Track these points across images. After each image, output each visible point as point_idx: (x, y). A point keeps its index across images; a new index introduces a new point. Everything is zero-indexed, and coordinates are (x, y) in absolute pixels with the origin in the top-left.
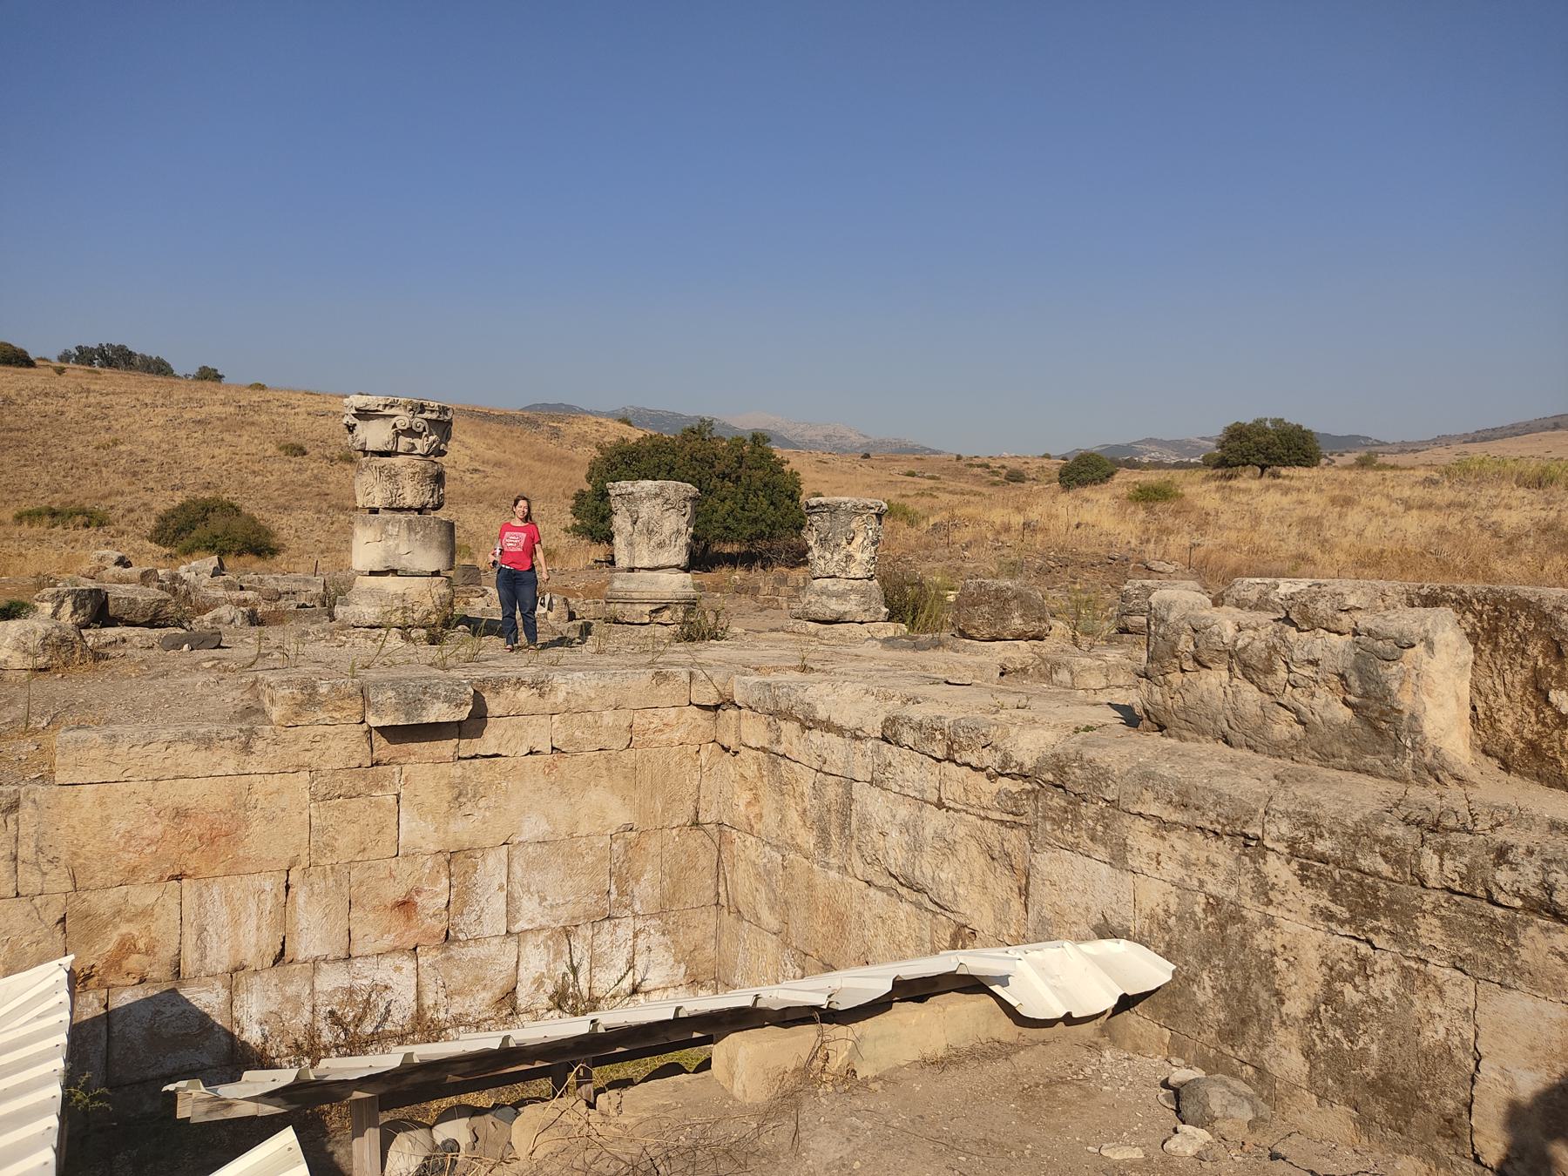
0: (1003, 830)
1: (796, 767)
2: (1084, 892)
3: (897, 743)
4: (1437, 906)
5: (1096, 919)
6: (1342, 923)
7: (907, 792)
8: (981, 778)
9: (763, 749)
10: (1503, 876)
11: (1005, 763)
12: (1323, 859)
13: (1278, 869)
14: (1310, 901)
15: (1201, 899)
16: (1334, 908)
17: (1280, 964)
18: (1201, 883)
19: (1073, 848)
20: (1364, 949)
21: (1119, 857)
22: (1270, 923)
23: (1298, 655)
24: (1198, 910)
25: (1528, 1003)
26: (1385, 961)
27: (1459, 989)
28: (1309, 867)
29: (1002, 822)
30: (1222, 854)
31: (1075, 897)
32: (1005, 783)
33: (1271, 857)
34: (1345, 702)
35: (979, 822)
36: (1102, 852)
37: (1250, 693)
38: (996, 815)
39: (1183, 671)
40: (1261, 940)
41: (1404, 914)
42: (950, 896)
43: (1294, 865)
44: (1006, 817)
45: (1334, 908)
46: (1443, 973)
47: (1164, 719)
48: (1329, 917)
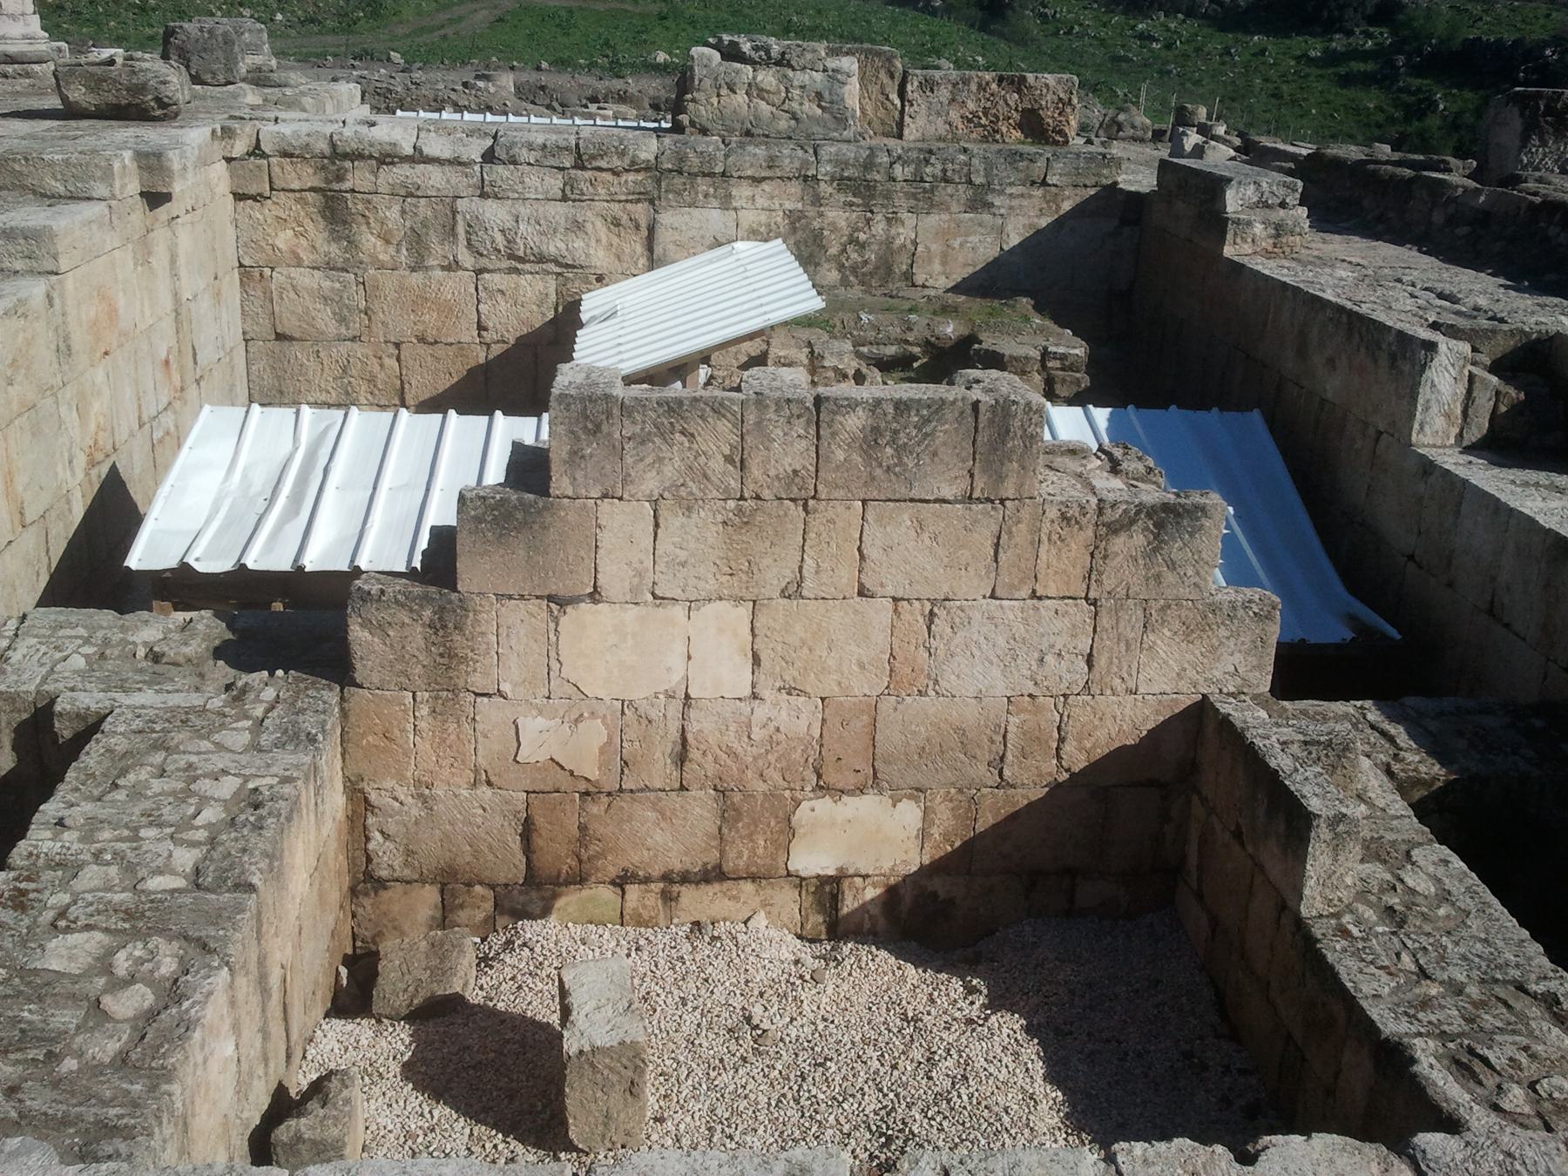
0: (629, 206)
1: (375, 198)
2: (700, 228)
3: (514, 162)
4: (902, 188)
5: (709, 240)
6: (858, 206)
7: (527, 196)
8: (608, 176)
9: (312, 189)
10: (928, 170)
11: (633, 163)
12: (849, 179)
13: (825, 189)
14: (842, 199)
15: (781, 214)
16: (855, 200)
17: (825, 233)
18: (781, 205)
20: (869, 215)
21: (726, 203)
22: (821, 215)
23: (796, 83)
24: (779, 219)
25: (937, 217)
26: (879, 217)
27: (910, 219)
28: (842, 182)
29: (627, 201)
30: (795, 188)
31: (694, 232)
32: (631, 177)
33: (822, 184)
34: (819, 106)
35: (606, 204)
36: (715, 203)
37: (763, 104)
38: (623, 198)
39: (719, 95)
40: (816, 224)
41: (888, 196)
42: (583, 258)
43: (835, 184)
44: (630, 197)
45: (855, 200)
46: (904, 215)
47: (709, 125)
48: (851, 204)
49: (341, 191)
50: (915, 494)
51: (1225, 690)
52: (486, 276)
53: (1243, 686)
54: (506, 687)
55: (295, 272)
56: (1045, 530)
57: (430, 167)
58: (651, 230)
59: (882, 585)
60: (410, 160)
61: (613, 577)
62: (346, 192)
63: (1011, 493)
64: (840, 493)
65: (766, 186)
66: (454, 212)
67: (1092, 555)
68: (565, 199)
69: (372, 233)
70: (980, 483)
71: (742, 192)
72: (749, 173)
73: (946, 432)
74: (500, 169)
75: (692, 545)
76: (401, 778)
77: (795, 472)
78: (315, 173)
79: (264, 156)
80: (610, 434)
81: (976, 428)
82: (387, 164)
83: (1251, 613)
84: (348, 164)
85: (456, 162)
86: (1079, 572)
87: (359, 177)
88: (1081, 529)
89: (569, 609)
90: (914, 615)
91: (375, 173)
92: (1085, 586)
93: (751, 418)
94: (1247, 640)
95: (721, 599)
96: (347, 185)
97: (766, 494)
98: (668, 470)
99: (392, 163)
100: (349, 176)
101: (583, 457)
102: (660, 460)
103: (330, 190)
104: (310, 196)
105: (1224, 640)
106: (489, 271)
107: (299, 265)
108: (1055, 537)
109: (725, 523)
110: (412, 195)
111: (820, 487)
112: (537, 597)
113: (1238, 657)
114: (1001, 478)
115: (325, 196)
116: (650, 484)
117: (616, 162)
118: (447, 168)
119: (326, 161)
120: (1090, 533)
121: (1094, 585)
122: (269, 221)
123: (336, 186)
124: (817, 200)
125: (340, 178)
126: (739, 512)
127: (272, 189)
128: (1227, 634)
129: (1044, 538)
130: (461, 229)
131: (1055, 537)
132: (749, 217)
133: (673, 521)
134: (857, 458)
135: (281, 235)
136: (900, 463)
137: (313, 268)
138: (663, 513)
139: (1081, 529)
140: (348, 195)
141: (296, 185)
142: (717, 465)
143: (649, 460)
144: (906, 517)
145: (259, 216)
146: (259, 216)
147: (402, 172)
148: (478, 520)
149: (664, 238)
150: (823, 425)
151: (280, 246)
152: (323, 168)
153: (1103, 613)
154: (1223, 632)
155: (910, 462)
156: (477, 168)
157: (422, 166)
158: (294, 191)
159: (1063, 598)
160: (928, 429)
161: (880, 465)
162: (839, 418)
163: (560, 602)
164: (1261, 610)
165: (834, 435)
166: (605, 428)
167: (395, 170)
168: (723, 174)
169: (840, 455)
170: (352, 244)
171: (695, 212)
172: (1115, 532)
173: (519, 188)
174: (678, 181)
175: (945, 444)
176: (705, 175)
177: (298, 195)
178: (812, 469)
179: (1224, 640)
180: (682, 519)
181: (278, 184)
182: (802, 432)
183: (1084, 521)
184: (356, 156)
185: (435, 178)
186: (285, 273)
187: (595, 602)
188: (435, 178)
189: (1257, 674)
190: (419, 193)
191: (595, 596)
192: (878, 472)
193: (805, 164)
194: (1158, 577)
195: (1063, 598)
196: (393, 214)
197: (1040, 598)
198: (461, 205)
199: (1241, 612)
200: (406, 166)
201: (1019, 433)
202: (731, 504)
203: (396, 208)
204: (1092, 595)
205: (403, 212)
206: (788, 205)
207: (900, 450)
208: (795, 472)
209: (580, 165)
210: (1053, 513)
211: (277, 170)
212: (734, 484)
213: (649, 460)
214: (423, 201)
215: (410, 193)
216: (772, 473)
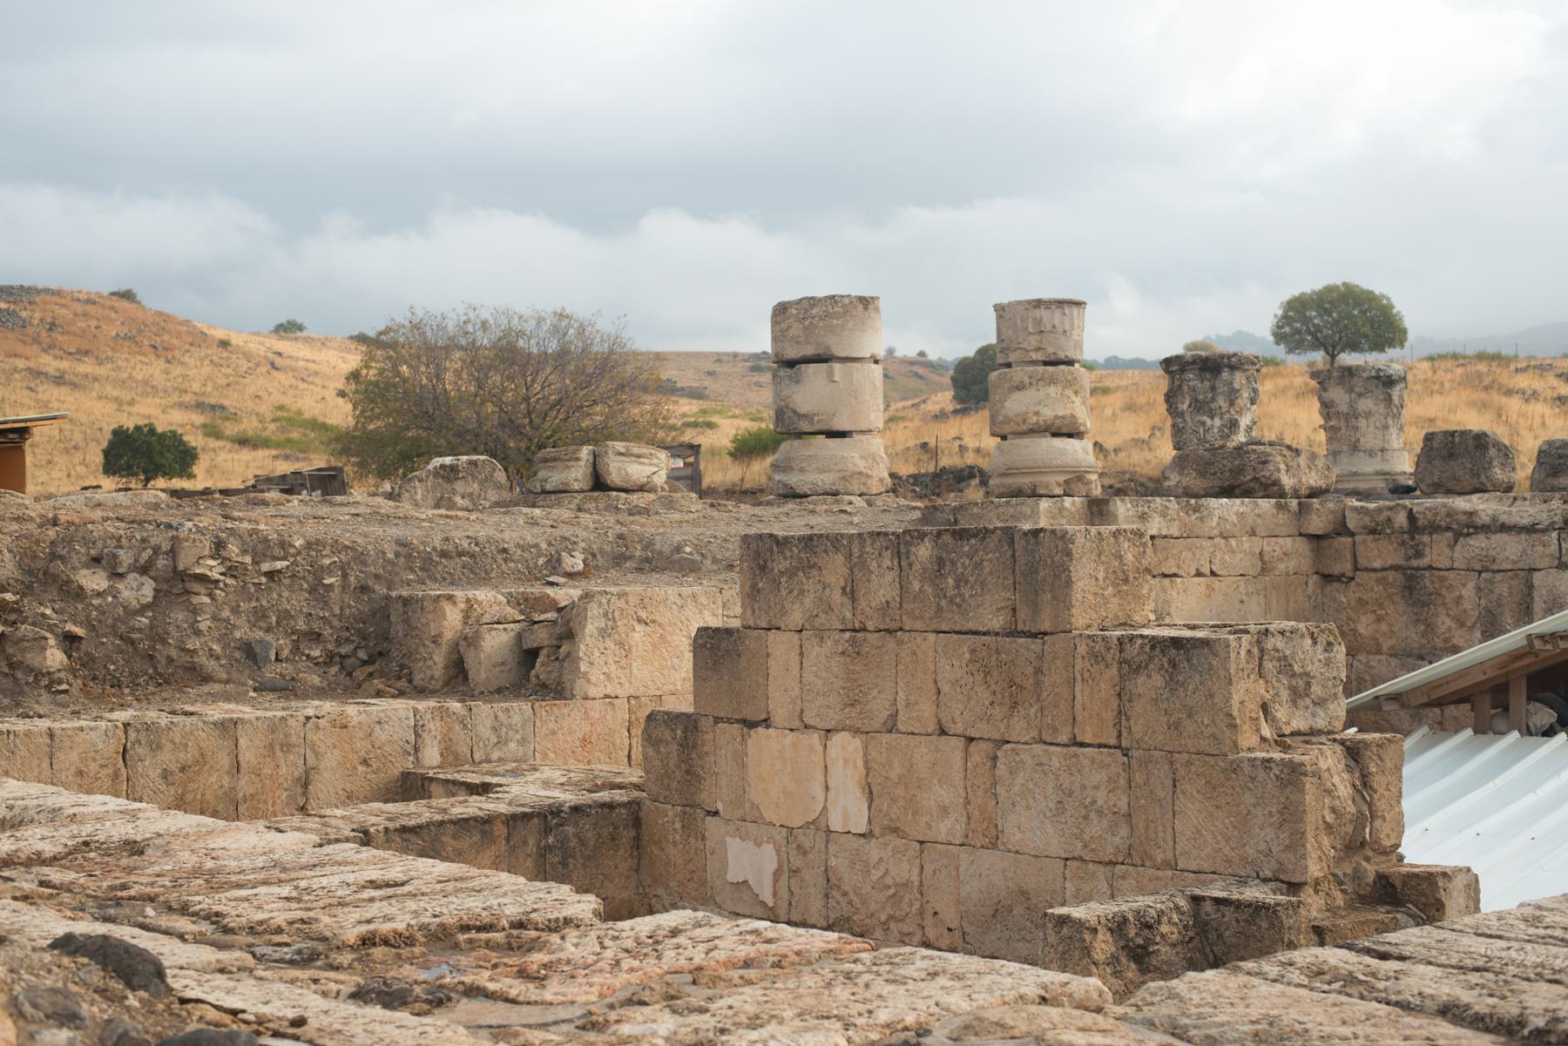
1: (1451, 575)
9: (1395, 568)
49: (1418, 569)
50: (971, 626)
51: (1261, 874)
53: (1278, 870)
54: (720, 806)
55: (1374, 660)
56: (1078, 668)
57: (1505, 537)
59: (954, 723)
60: (1486, 529)
61: (780, 704)
62: (1424, 569)
63: (1046, 626)
64: (918, 625)
66: (1531, 587)
67: (1119, 695)
69: (1448, 615)
70: (1023, 613)
73: (991, 561)
75: (824, 674)
76: (667, 888)
77: (887, 602)
78: (1395, 550)
79: (1352, 534)
80: (772, 569)
81: (1013, 555)
83: (1272, 775)
84: (1426, 539)
85: (1531, 529)
86: (1109, 715)
87: (1437, 551)
88: (1107, 666)
89: (752, 732)
90: (979, 752)
91: (1452, 547)
92: (1115, 733)
93: (855, 550)
94: (1273, 810)
95: (843, 729)
96: (1425, 561)
97: (870, 625)
98: (808, 601)
99: (1468, 535)
100: (1427, 550)
101: (758, 590)
102: (802, 592)
103: (1410, 568)
104: (1391, 575)
105: (1252, 809)
107: (1379, 652)
108: (1087, 675)
109: (843, 653)
110: (1487, 570)
111: (904, 617)
112: (738, 721)
113: (1269, 833)
114: (1035, 608)
115: (1404, 574)
116: (796, 617)
118: (1523, 536)
119: (1406, 536)
120: (1114, 670)
121: (1124, 733)
122: (1353, 603)
123: (1415, 563)
125: (1419, 554)
126: (853, 639)
127: (1356, 568)
128: (1252, 800)
129: (1078, 676)
131: (1087, 675)
133: (815, 651)
134: (928, 589)
135: (1363, 619)
136: (961, 595)
137: (1391, 655)
138: (806, 644)
139: (1107, 666)
140: (1427, 573)
141: (1377, 564)
142: (837, 597)
143: (795, 592)
144: (965, 649)
145: (1343, 599)
146: (1343, 599)
147: (1479, 542)
148: (704, 646)
150: (903, 557)
151: (1362, 631)
152: (1403, 543)
153: (1134, 762)
154: (1249, 799)
155: (966, 592)
156: (1555, 535)
157: (1498, 536)
158: (1374, 570)
159: (1100, 746)
160: (976, 559)
161: (945, 597)
162: (913, 549)
163: (751, 724)
164: (1282, 771)
165: (910, 565)
166: (769, 564)
167: (1471, 542)
169: (916, 586)
170: (1430, 628)
172: (1137, 671)
175: (991, 573)
177: (1380, 575)
178: (898, 599)
179: (1252, 809)
180: (818, 649)
181: (1363, 562)
182: (889, 563)
183: (1109, 658)
184: (1434, 528)
185: (1509, 549)
186: (1364, 660)
187: (768, 727)
189: (1291, 856)
190: (1495, 567)
191: (766, 722)
192: (943, 603)
194: (1177, 726)
195: (1100, 746)
196: (1468, 592)
197: (1082, 745)
198: (1537, 578)
199: (1261, 774)
200: (1482, 537)
201: (1049, 561)
202: (847, 635)
203: (1471, 585)
204: (1123, 745)
205: (1479, 589)
207: (961, 581)
208: (887, 602)
210: (1082, 649)
211: (1360, 548)
212: (849, 615)
213: (795, 592)
214: (1499, 577)
215: (1484, 568)
216: (873, 604)
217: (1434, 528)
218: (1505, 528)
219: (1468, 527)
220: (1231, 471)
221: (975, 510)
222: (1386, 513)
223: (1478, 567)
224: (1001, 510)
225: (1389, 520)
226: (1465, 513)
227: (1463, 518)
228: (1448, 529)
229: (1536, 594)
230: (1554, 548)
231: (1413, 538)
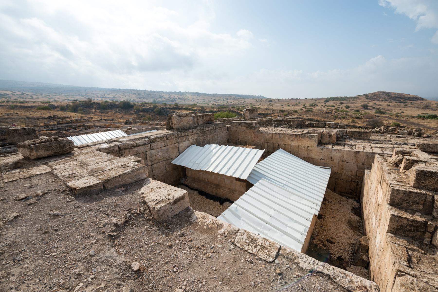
13: (199, 134)
19: (184, 141)
30: (196, 135)
41: (206, 133)
52: (154, 165)
57: (140, 147)
58: (178, 148)
65: (193, 136)
66: (146, 155)
68: (165, 146)
71: (190, 137)
72: (190, 134)
74: (154, 144)
82: (131, 149)
84: (123, 151)
85: (145, 144)
100: (124, 153)
106: (153, 164)
110: (138, 154)
117: (173, 137)
118: (144, 146)
124: (199, 136)
130: (148, 158)
132: (191, 141)
147: (135, 149)
149: (181, 148)
156: (149, 144)
168: (187, 135)
171: (184, 142)
173: (157, 146)
174: (181, 138)
176: (185, 136)
184: (125, 149)
188: (142, 149)
193: (197, 131)
198: (147, 153)
206: (196, 138)
209: (167, 139)
217: (125, 149)
218: (140, 145)
219: (133, 147)
220: (60, 147)
221: (117, 179)
222: (112, 148)
223: (136, 154)
224: (130, 175)
225: (113, 149)
226: (132, 144)
227: (132, 145)
228: (128, 148)
229: (148, 156)
230: (150, 147)
231: (120, 152)
